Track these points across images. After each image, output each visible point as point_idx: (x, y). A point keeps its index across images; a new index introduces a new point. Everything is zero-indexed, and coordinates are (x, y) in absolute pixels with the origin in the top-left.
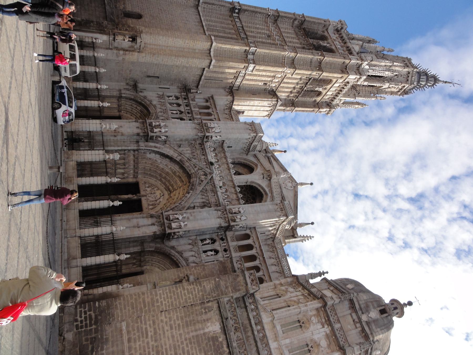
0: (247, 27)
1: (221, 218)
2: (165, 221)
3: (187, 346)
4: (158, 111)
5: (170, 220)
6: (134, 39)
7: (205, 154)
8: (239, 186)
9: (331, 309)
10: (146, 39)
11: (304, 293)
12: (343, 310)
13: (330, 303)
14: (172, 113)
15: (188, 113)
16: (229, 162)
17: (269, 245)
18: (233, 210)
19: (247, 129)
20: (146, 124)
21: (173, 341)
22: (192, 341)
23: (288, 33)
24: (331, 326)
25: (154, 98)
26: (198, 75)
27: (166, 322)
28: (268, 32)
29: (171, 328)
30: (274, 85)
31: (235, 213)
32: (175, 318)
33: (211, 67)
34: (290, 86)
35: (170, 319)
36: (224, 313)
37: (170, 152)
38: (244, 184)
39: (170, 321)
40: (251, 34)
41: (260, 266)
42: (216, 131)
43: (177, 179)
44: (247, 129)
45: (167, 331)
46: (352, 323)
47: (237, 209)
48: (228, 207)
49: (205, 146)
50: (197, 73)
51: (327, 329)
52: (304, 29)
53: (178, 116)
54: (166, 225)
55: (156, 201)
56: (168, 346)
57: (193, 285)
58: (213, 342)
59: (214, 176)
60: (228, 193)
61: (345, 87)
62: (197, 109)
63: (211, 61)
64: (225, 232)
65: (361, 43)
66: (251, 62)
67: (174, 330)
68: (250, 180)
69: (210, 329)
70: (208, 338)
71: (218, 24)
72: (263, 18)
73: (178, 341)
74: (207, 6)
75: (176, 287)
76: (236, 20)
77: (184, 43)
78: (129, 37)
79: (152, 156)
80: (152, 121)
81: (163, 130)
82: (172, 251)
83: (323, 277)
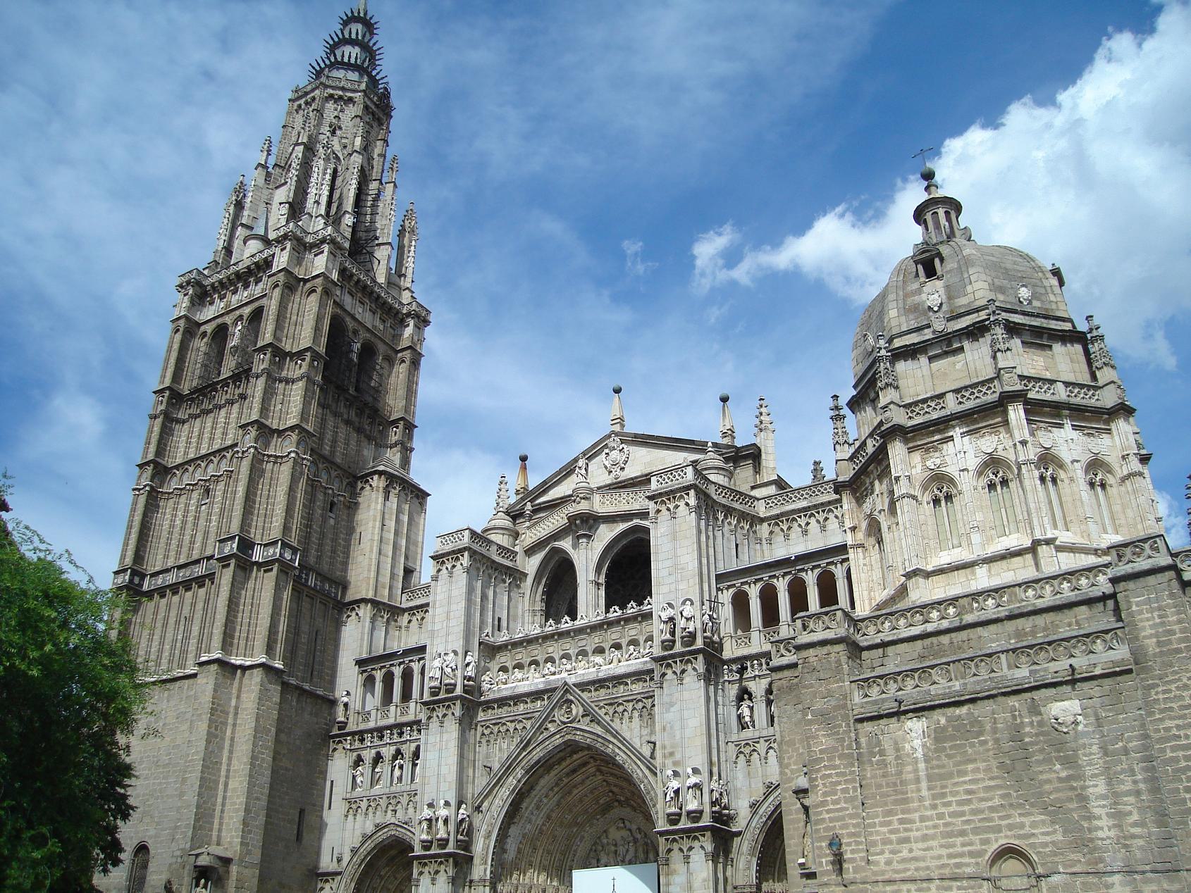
0: (178, 553)
1: (683, 671)
2: (680, 826)
3: (949, 804)
4: (393, 820)
5: (680, 815)
7: (517, 699)
8: (607, 611)
9: (913, 411)
11: (876, 474)
12: (916, 379)
13: (899, 417)
14: (400, 779)
15: (401, 734)
16: (538, 631)
17: (771, 532)
18: (664, 637)
19: (451, 574)
20: (424, 857)
21: (933, 837)
22: (938, 791)
23: (200, 437)
24: (951, 420)
25: (358, 825)
26: (298, 701)
27: (892, 852)
28: (195, 495)
29: (906, 840)
31: (673, 633)
32: (885, 829)
33: (278, 665)
34: (341, 436)
35: (886, 842)
36: (891, 706)
37: (504, 795)
38: (602, 592)
39: (891, 842)
40: (198, 545)
41: (817, 571)
42: (453, 665)
43: (578, 778)
44: (451, 574)
45: (911, 851)
46: (951, 359)
47: (662, 626)
48: (657, 651)
49: (491, 696)
51: (956, 432)
52: (192, 393)
53: (408, 767)
54: (690, 825)
55: (635, 841)
56: (944, 852)
57: (816, 779)
58: (945, 739)
59: (572, 680)
60: (624, 642)
61: (355, 278)
62: (392, 708)
64: (725, 662)
65: (240, 232)
66: (271, 551)
67: (912, 834)
68: (592, 577)
69: (917, 743)
70: (936, 750)
71: (169, 635)
73: (935, 827)
75: (818, 822)
76: (160, 582)
77: (216, 737)
79: (511, 846)
80: (417, 841)
81: (443, 812)
82: (761, 811)
83: (846, 411)
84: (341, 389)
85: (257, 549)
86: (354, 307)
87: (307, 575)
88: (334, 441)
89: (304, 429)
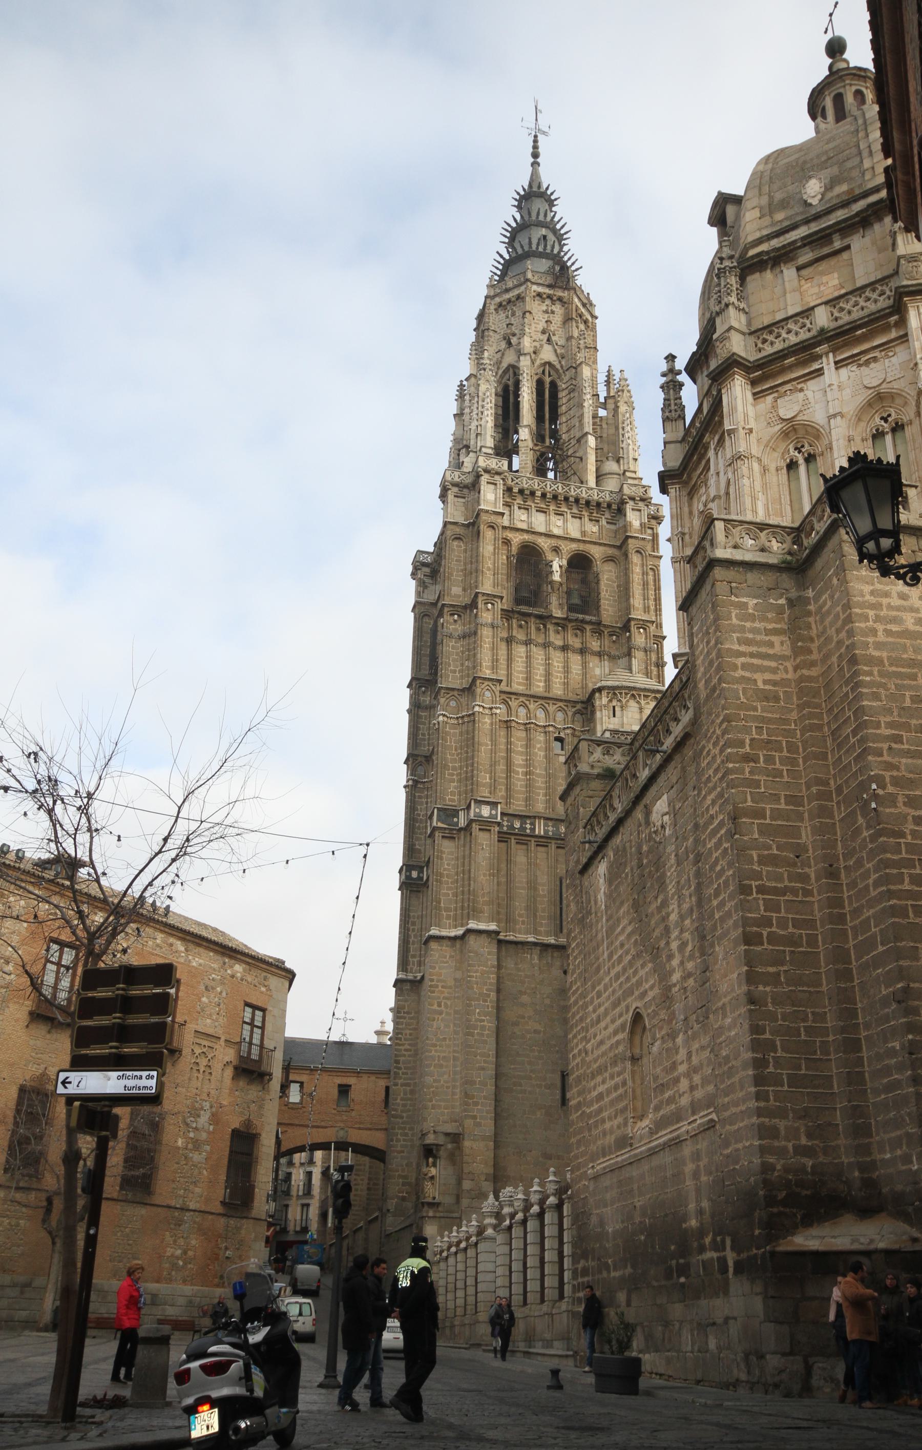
6: (429, 1152)
10: (437, 1119)
26: (540, 958)
30: (560, 716)
33: (493, 927)
50: (536, 961)
61: (539, 494)
63: (469, 931)
72: (427, 797)
74: (414, 956)
77: (441, 1013)
78: (427, 1165)
84: (544, 619)
85: (461, 814)
86: (548, 523)
87: (533, 824)
88: (548, 675)
89: (485, 679)
